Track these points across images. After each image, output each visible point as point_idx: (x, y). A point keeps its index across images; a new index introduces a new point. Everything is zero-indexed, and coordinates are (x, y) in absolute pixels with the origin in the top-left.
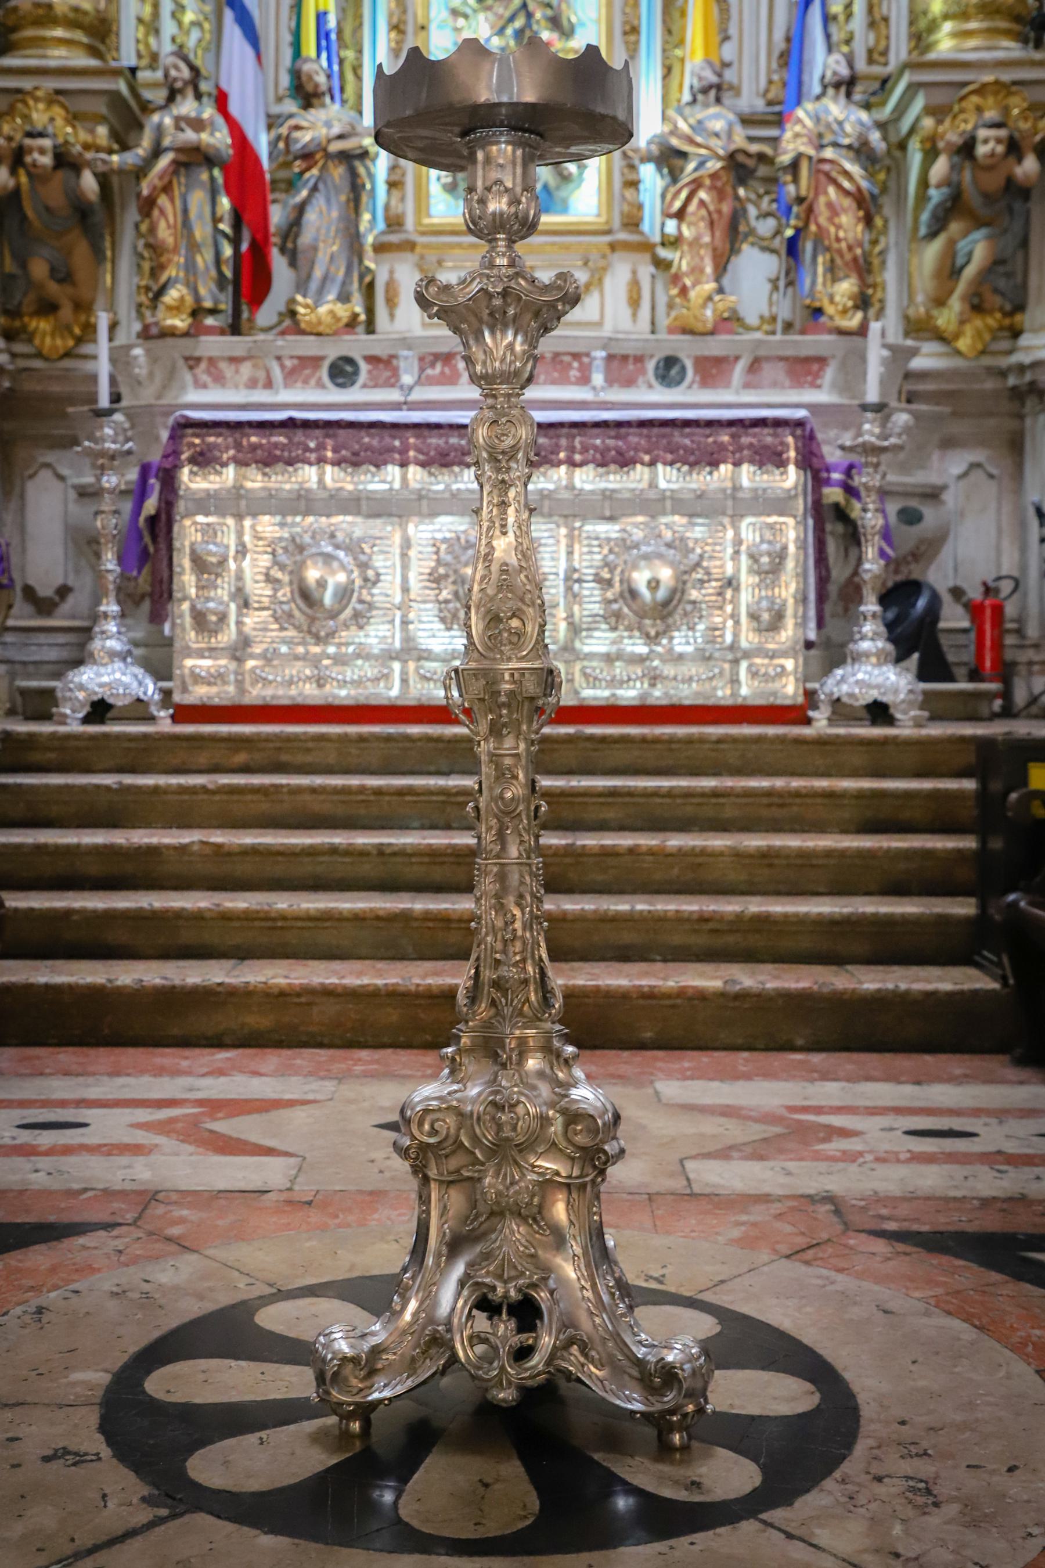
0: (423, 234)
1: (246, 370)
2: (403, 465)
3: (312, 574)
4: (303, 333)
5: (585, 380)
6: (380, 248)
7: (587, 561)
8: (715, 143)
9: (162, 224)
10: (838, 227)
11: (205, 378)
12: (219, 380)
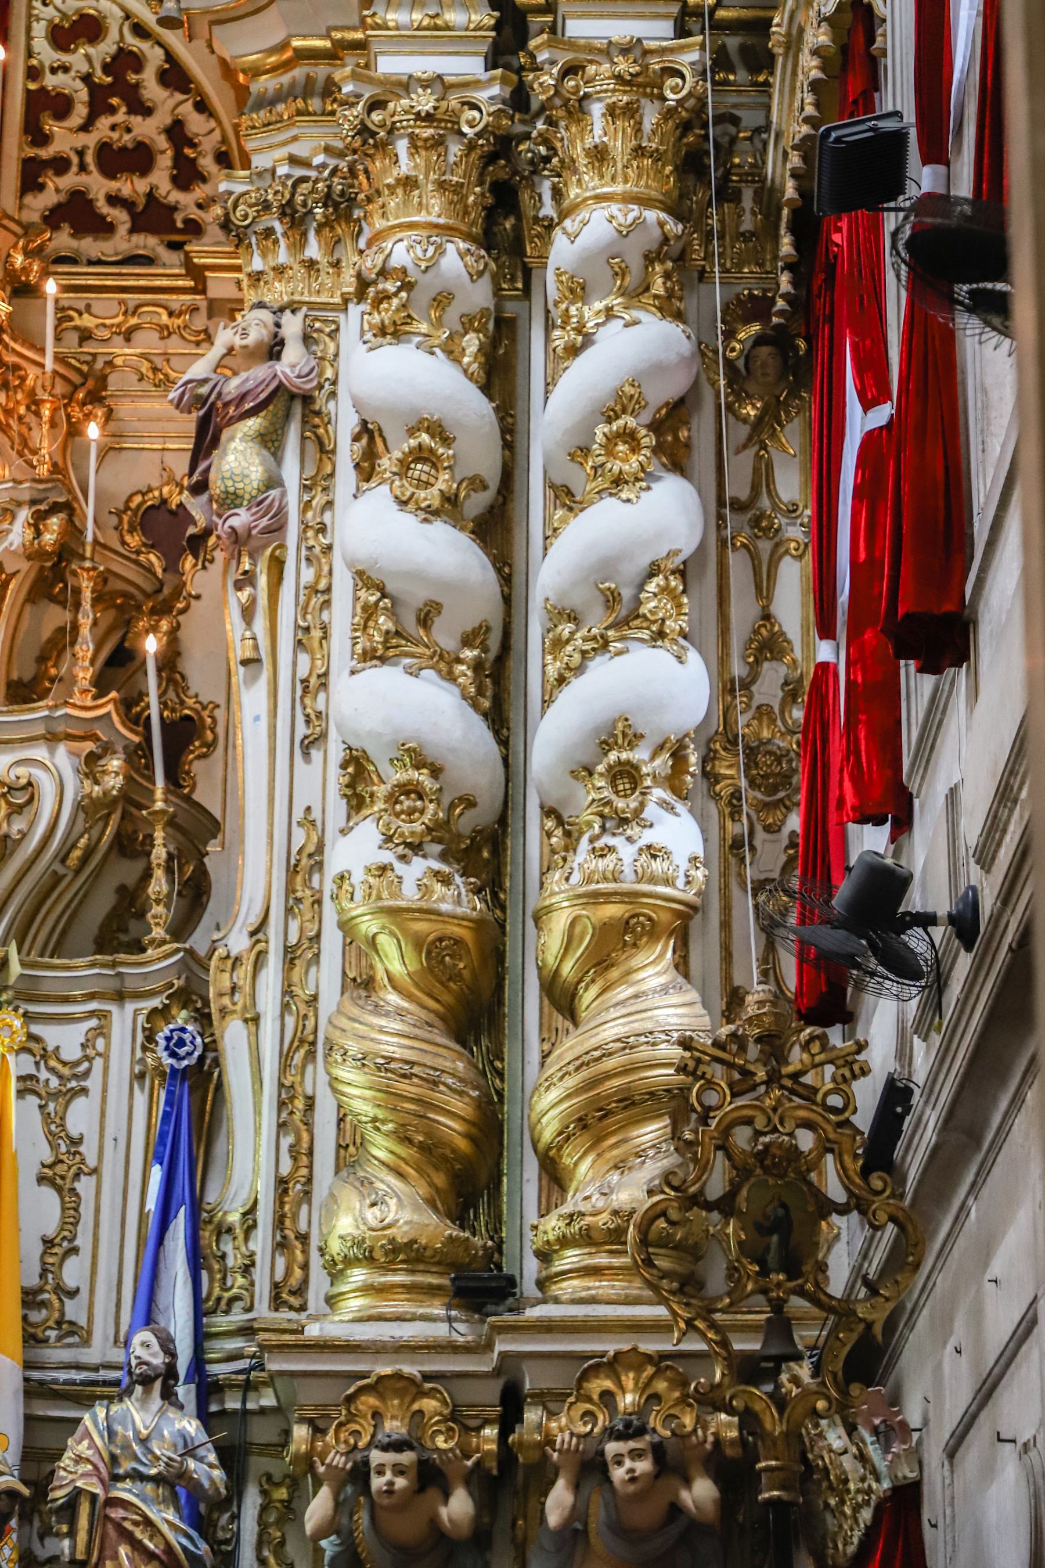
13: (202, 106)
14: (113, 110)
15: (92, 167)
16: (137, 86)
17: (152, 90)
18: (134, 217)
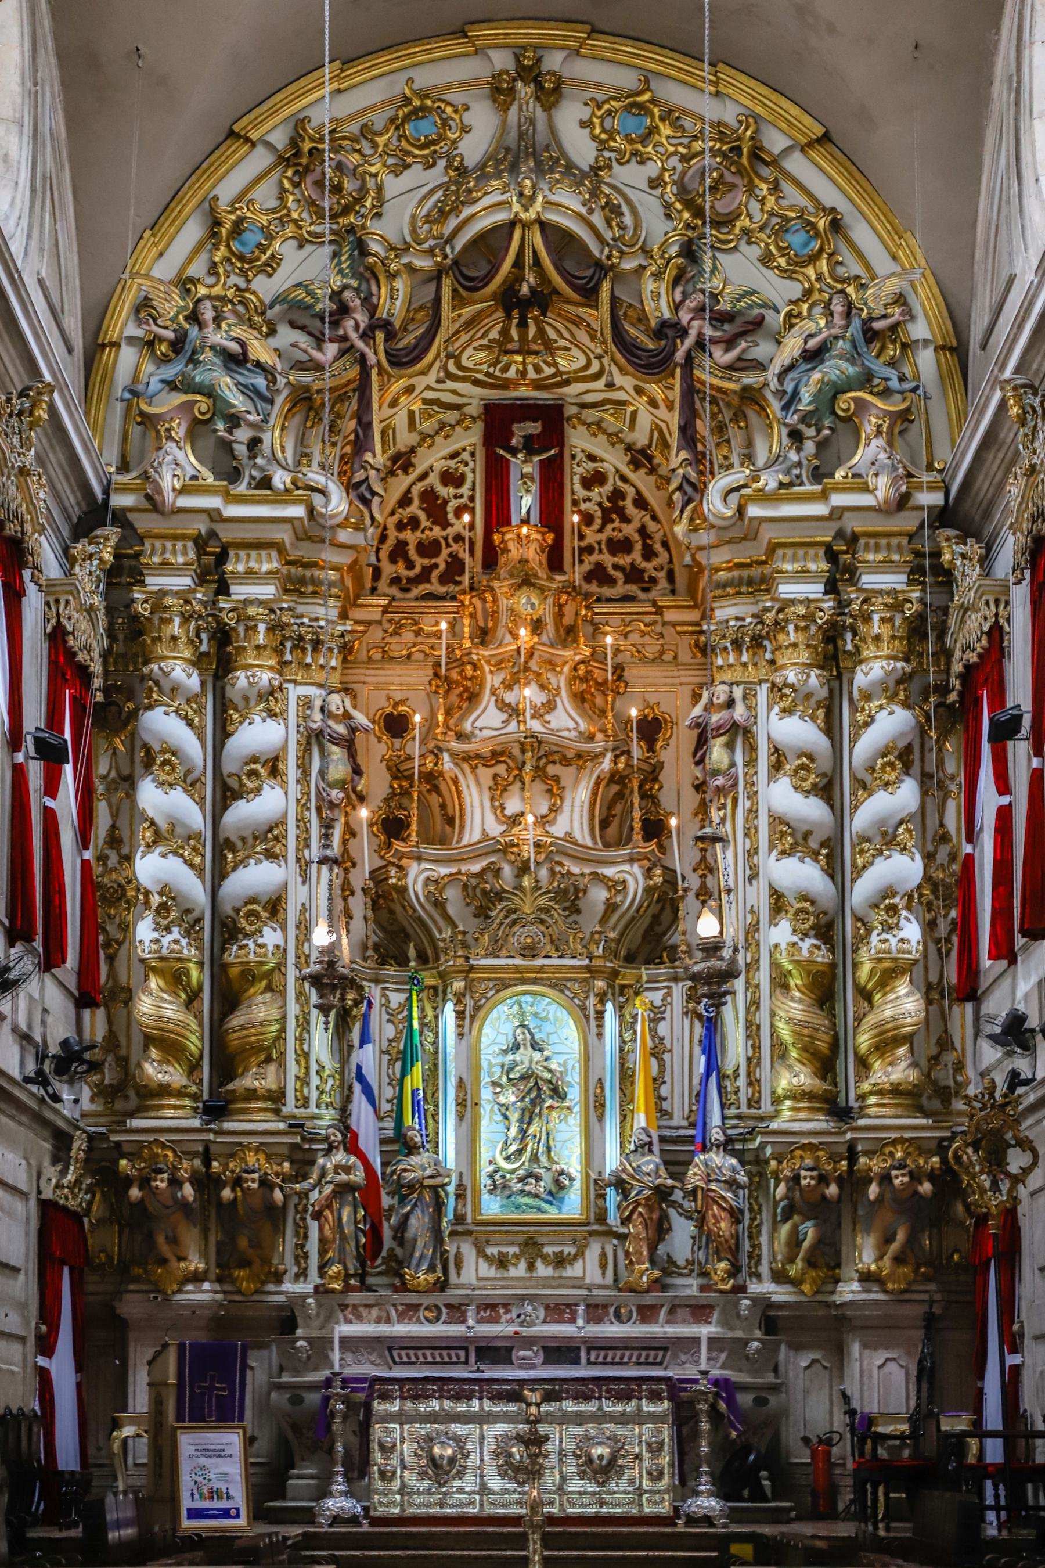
0: (477, 1225)
1: (375, 1312)
2: (481, 1399)
3: (437, 1450)
4: (409, 1291)
5: (573, 1320)
6: (452, 1234)
7: (570, 1446)
8: (646, 1179)
9: (327, 1227)
10: (720, 1229)
11: (351, 1316)
12: (359, 1318)
13: (654, 518)
14: (613, 521)
15: (605, 551)
16: (623, 508)
17: (631, 510)
18: (626, 575)
